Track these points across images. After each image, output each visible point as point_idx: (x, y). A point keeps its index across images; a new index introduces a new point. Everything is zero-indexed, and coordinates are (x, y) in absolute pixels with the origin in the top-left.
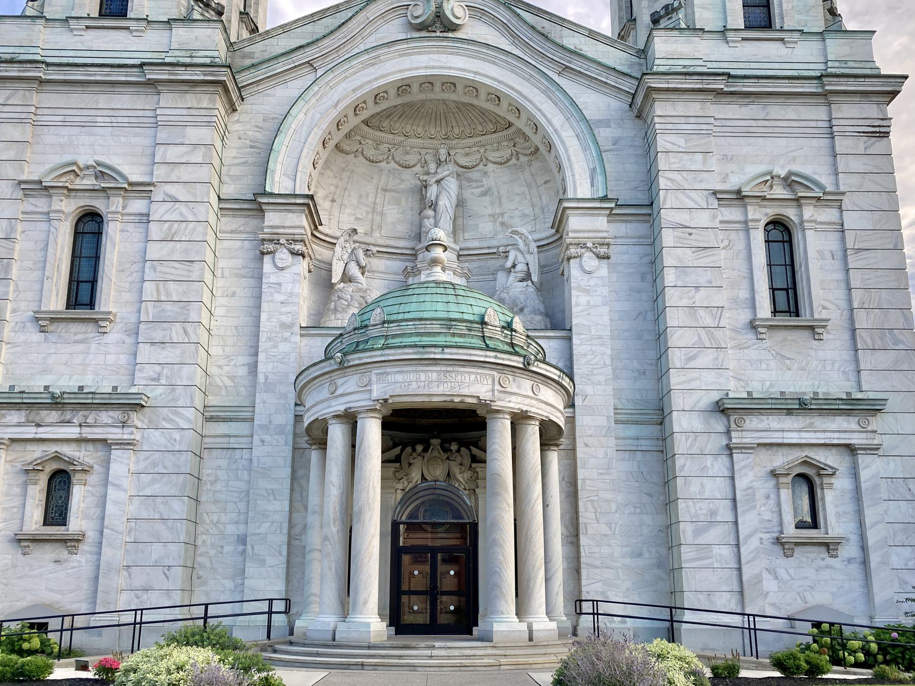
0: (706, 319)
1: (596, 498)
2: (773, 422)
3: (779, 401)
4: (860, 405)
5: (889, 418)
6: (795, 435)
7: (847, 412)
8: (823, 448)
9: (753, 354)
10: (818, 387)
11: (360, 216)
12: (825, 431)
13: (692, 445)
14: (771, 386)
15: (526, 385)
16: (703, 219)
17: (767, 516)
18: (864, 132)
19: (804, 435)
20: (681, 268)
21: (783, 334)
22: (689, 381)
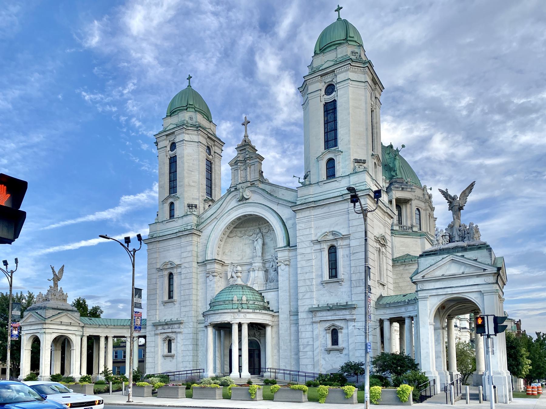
2: (324, 313)
9: (321, 292)
16: (308, 250)
17: (324, 342)
20: (302, 268)
21: (330, 285)
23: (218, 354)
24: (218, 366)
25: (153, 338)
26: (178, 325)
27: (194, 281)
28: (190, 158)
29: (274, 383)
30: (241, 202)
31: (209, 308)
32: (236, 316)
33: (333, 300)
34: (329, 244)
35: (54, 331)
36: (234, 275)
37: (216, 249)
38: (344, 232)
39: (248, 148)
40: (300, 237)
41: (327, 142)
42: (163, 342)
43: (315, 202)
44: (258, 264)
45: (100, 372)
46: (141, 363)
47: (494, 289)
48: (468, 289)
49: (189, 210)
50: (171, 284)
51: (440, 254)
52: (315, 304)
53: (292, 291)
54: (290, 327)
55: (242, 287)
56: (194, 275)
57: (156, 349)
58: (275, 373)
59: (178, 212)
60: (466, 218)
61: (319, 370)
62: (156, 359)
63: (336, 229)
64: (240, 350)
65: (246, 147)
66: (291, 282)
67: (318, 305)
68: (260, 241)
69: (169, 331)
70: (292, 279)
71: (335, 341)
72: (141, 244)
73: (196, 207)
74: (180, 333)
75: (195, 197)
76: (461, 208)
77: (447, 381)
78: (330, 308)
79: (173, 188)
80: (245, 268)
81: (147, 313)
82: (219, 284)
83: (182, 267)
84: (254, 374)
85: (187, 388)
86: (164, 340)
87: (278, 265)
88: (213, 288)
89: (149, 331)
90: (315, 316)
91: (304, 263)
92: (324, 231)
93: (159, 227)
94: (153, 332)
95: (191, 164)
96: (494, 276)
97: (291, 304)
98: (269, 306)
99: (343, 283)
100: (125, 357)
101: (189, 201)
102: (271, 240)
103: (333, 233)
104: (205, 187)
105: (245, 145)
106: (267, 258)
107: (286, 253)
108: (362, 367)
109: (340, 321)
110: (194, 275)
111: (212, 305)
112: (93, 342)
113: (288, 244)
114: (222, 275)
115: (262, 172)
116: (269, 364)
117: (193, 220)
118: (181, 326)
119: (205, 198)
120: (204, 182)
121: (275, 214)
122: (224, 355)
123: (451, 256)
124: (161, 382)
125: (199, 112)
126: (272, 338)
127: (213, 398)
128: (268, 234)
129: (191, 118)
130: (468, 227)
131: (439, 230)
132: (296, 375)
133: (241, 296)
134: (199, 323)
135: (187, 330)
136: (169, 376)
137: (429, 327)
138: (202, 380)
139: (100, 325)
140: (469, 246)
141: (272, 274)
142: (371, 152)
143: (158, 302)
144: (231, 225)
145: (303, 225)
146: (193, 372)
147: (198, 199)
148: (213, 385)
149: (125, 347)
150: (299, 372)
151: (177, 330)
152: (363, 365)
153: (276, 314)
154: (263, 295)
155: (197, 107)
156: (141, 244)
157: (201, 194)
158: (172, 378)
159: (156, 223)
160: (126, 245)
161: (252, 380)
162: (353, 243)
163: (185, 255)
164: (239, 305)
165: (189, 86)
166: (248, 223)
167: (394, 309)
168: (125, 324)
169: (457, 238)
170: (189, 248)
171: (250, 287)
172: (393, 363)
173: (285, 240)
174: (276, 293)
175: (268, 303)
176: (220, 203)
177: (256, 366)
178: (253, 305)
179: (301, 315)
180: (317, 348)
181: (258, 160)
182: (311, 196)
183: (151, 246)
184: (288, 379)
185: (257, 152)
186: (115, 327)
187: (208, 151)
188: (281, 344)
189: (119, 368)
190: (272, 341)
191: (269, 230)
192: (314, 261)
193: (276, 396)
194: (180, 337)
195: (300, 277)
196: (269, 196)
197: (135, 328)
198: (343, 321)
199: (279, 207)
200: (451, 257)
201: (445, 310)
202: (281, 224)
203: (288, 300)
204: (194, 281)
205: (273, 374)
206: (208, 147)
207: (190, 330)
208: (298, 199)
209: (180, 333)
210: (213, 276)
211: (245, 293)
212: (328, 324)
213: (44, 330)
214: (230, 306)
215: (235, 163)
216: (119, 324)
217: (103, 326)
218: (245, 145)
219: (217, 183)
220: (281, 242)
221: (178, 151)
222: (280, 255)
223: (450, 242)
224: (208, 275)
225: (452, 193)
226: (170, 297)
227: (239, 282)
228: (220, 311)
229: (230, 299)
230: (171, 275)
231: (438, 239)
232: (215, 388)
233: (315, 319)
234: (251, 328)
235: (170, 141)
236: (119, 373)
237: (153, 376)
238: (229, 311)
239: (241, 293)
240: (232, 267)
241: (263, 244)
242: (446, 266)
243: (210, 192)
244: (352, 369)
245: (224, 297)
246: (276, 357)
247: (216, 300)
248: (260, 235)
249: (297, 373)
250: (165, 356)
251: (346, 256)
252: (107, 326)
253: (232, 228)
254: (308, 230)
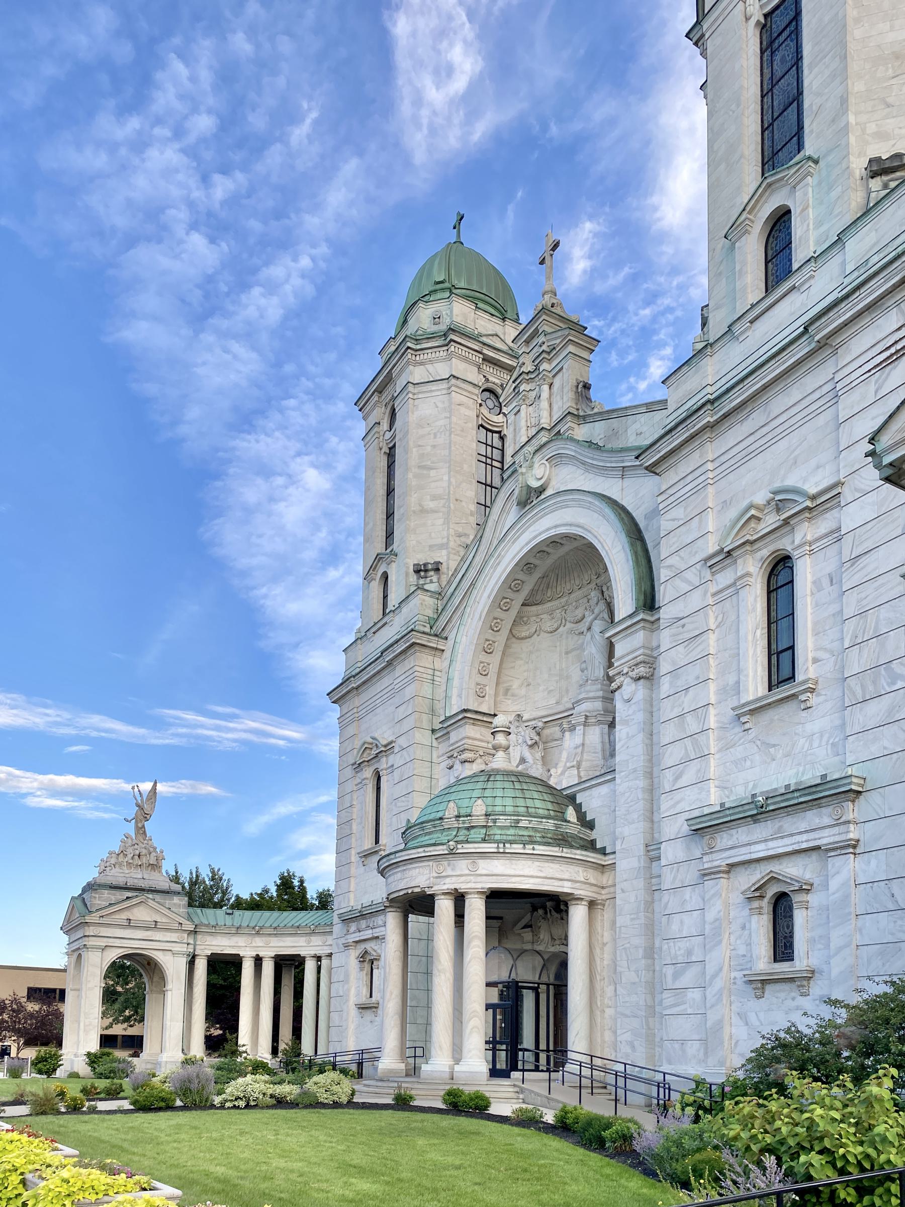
1: (628, 945)
2: (741, 834)
3: (737, 810)
4: (820, 791)
7: (816, 803)
8: (803, 855)
10: (803, 774)
11: (552, 688)
12: (792, 835)
13: (674, 879)
14: (755, 786)
15: (463, 866)
18: (875, 367)
19: (771, 844)
22: (674, 806)
52: (714, 798)
67: (722, 805)
78: (759, 811)
90: (711, 850)
99: (814, 700)
178: (512, 831)
179: (671, 852)
229: (440, 815)
233: (708, 863)
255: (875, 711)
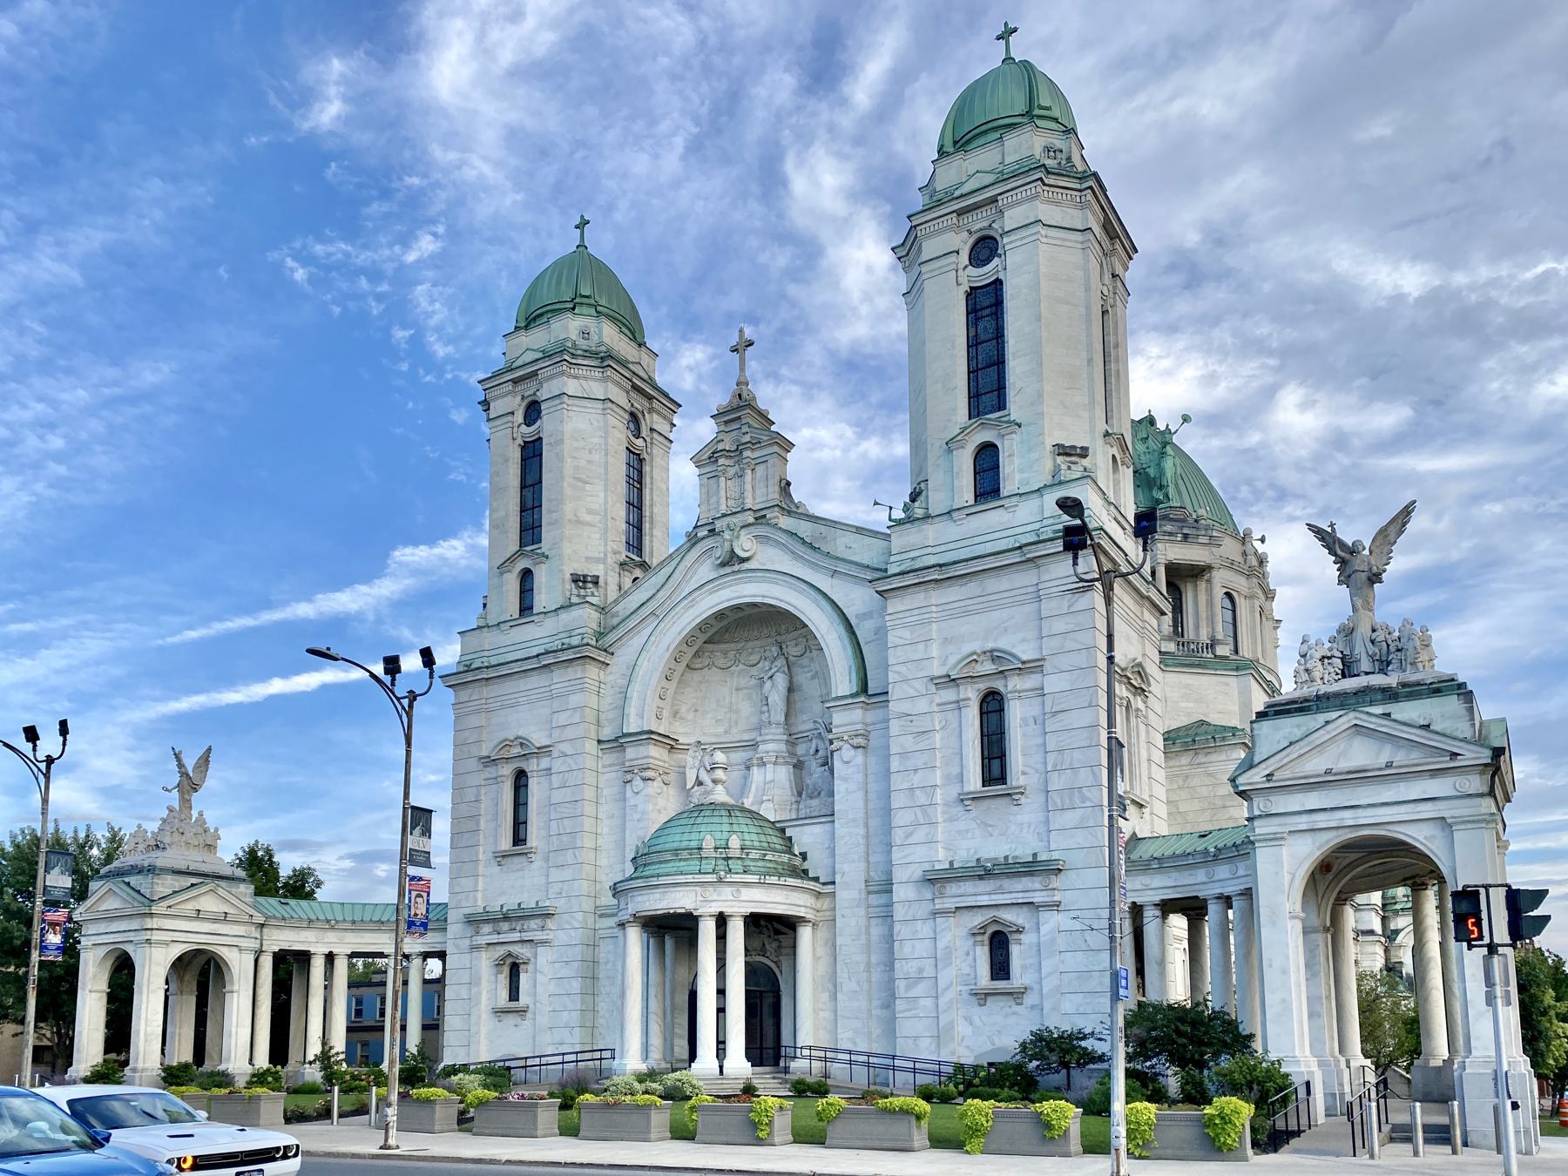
0: (922, 798)
2: (968, 887)
5: (1072, 875)
6: (986, 897)
7: (1030, 874)
9: (961, 825)
16: (922, 705)
17: (967, 970)
20: (904, 755)
21: (987, 803)
23: (654, 1005)
24: (656, 1041)
25: (466, 959)
26: (539, 921)
27: (589, 793)
28: (582, 443)
29: (821, 1090)
30: (728, 570)
31: (629, 870)
32: (711, 893)
33: (995, 849)
34: (983, 686)
35: (177, 936)
36: (704, 777)
37: (652, 703)
38: (1026, 652)
39: (748, 417)
40: (896, 668)
41: (975, 397)
42: (494, 970)
43: (940, 566)
44: (773, 745)
45: (310, 1057)
46: (430, 1033)
47: (1483, 811)
48: (1400, 812)
49: (575, 591)
50: (520, 804)
51: (1319, 710)
52: (941, 858)
53: (874, 822)
54: (868, 927)
55: (730, 810)
56: (590, 778)
57: (474, 990)
58: (825, 1060)
59: (543, 596)
60: (1391, 608)
61: (953, 1053)
62: (473, 1019)
63: (1003, 643)
64: (721, 992)
65: (741, 413)
66: (872, 796)
67: (951, 863)
68: (781, 681)
69: (511, 937)
70: (873, 787)
71: (1000, 968)
72: (431, 676)
73: (596, 583)
74: (544, 942)
75: (595, 555)
76: (1375, 578)
77: (1341, 1085)
78: (984, 872)
79: (530, 530)
80: (739, 757)
81: (451, 885)
82: (661, 802)
83: (555, 754)
84: (761, 1065)
85: (565, 1107)
86: (499, 965)
87: (833, 747)
88: (644, 813)
89: (454, 938)
90: (942, 895)
91: (908, 742)
92: (968, 648)
93: (489, 639)
94: (467, 942)
95: (583, 463)
96: (1482, 773)
97: (872, 859)
98: (806, 866)
100: (382, 1014)
101: (575, 565)
102: (813, 678)
103: (995, 656)
104: (624, 526)
105: (739, 408)
106: (802, 727)
107: (857, 714)
108: (1083, 1044)
109: (1015, 909)
110: (590, 778)
111: (640, 862)
112: (289, 969)
113: (864, 688)
114: (671, 778)
115: (788, 484)
116: (805, 1038)
117: (585, 619)
118: (550, 923)
119: (623, 558)
120: (620, 511)
121: (824, 602)
122: (674, 1008)
123: (1352, 715)
124: (486, 1086)
125: (607, 316)
126: (816, 958)
127: (643, 1136)
128: (805, 661)
129: (585, 334)
130: (1397, 634)
131: (1312, 641)
132: (886, 1068)
133: (725, 835)
134: (601, 916)
135: (565, 935)
136: (509, 1068)
137: (1289, 924)
138: (607, 1083)
139: (310, 921)
140: (1404, 685)
141: (815, 772)
142: (1102, 427)
143: (484, 853)
144: (698, 634)
145: (906, 634)
146: (580, 1057)
147: (604, 561)
148: (642, 1099)
149: (384, 984)
150: (893, 1057)
151: (538, 936)
152: (1084, 1038)
153: (829, 889)
154: (788, 834)
155: (603, 302)
156: (431, 676)
157: (611, 545)
158: (518, 1074)
159: (479, 628)
160: (387, 679)
161: (755, 1082)
162: (1053, 683)
163: (562, 719)
164: (720, 862)
165: (582, 246)
166: (749, 629)
167: (1175, 875)
168: (384, 919)
169: (1365, 665)
170: (575, 700)
171: (750, 812)
172: (1180, 1033)
173: (854, 675)
174: (827, 827)
175: (804, 856)
176: (667, 571)
177: (766, 1043)
178: (760, 864)
180: (946, 989)
181: (776, 449)
182: (930, 550)
183: (464, 695)
184: (861, 1078)
185: (773, 428)
186: (356, 925)
187: (632, 426)
188: (842, 975)
189: (365, 1044)
190: (815, 969)
191: (807, 649)
192: (938, 736)
193: (833, 1132)
194: (544, 957)
195: (897, 782)
196: (810, 551)
197: (411, 924)
198: (1025, 908)
199: (836, 582)
200: (1350, 718)
201: (1330, 876)
202: (842, 630)
203: (862, 849)
204: (589, 793)
205: (816, 1065)
206: (632, 414)
207: (576, 936)
208: (893, 559)
209: (544, 942)
210: (645, 779)
211: (735, 828)
212: (979, 919)
213: (147, 935)
214: (694, 865)
215: (709, 459)
216: (367, 918)
217: (319, 925)
218: (739, 408)
219: (657, 518)
220: (843, 682)
221: (547, 425)
222: (838, 718)
223: (1344, 676)
224: (629, 777)
225: (1347, 536)
226: (519, 839)
227: (720, 795)
228: (663, 880)
229: (694, 844)
230: (521, 779)
231: (1309, 666)
232: (647, 1107)
233: (940, 904)
234: (752, 928)
235: (523, 398)
236: (366, 1060)
237: (464, 1068)
238: (689, 878)
239: (726, 827)
240: (699, 754)
241: (790, 690)
242: (1339, 745)
243: (636, 543)
244: (1051, 1050)
245: (675, 839)
246: (827, 1014)
247: (653, 849)
248: (781, 662)
249: (889, 1062)
250: (500, 1012)
251: (1031, 721)
252: (331, 925)
253: (700, 642)
254: (921, 646)
255: (1070, 818)
